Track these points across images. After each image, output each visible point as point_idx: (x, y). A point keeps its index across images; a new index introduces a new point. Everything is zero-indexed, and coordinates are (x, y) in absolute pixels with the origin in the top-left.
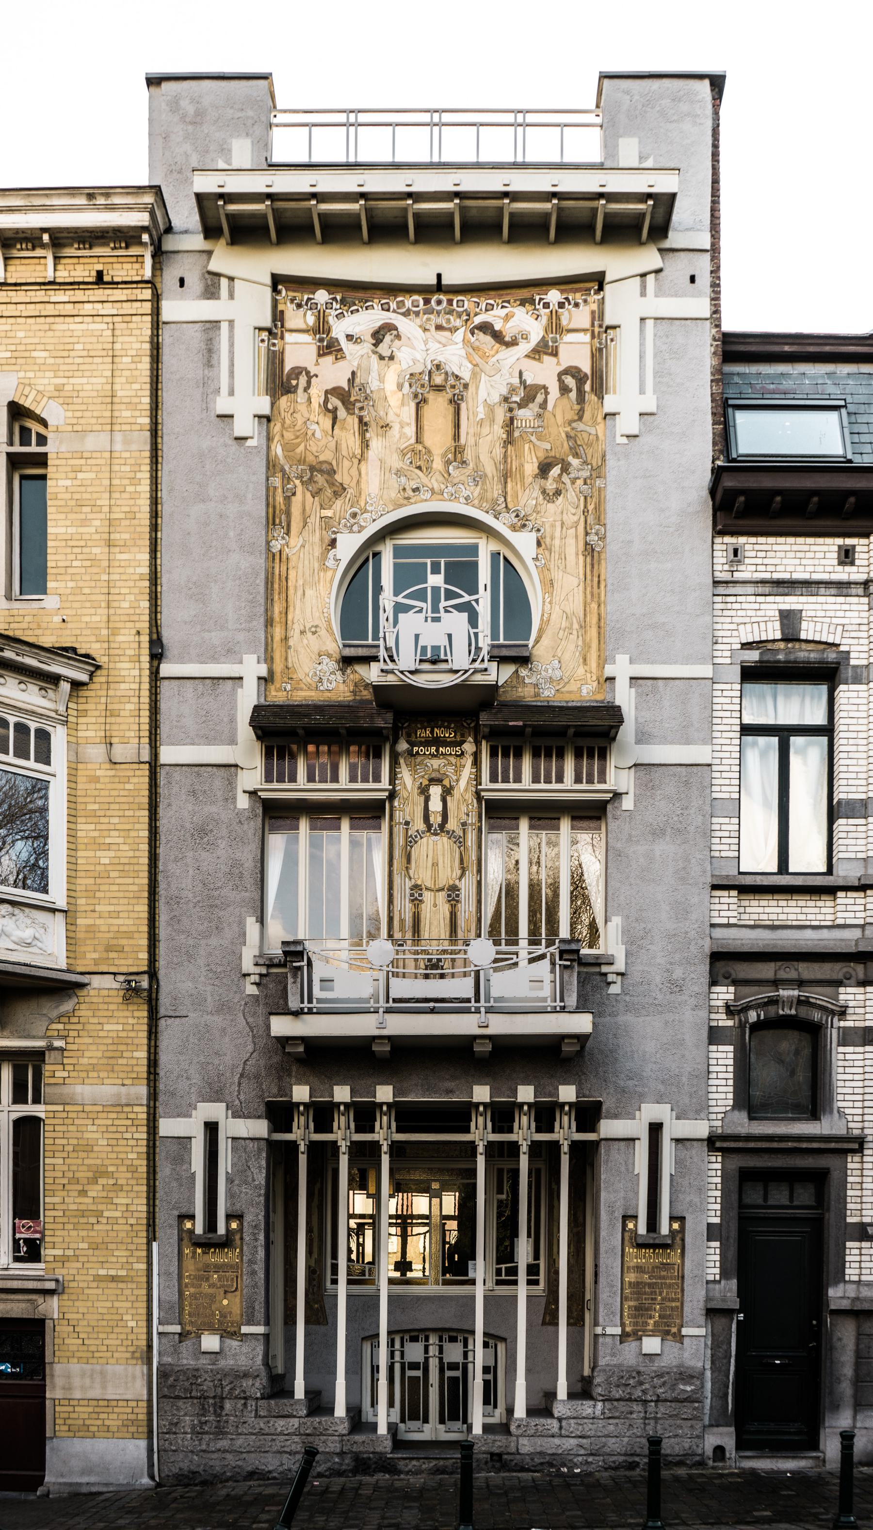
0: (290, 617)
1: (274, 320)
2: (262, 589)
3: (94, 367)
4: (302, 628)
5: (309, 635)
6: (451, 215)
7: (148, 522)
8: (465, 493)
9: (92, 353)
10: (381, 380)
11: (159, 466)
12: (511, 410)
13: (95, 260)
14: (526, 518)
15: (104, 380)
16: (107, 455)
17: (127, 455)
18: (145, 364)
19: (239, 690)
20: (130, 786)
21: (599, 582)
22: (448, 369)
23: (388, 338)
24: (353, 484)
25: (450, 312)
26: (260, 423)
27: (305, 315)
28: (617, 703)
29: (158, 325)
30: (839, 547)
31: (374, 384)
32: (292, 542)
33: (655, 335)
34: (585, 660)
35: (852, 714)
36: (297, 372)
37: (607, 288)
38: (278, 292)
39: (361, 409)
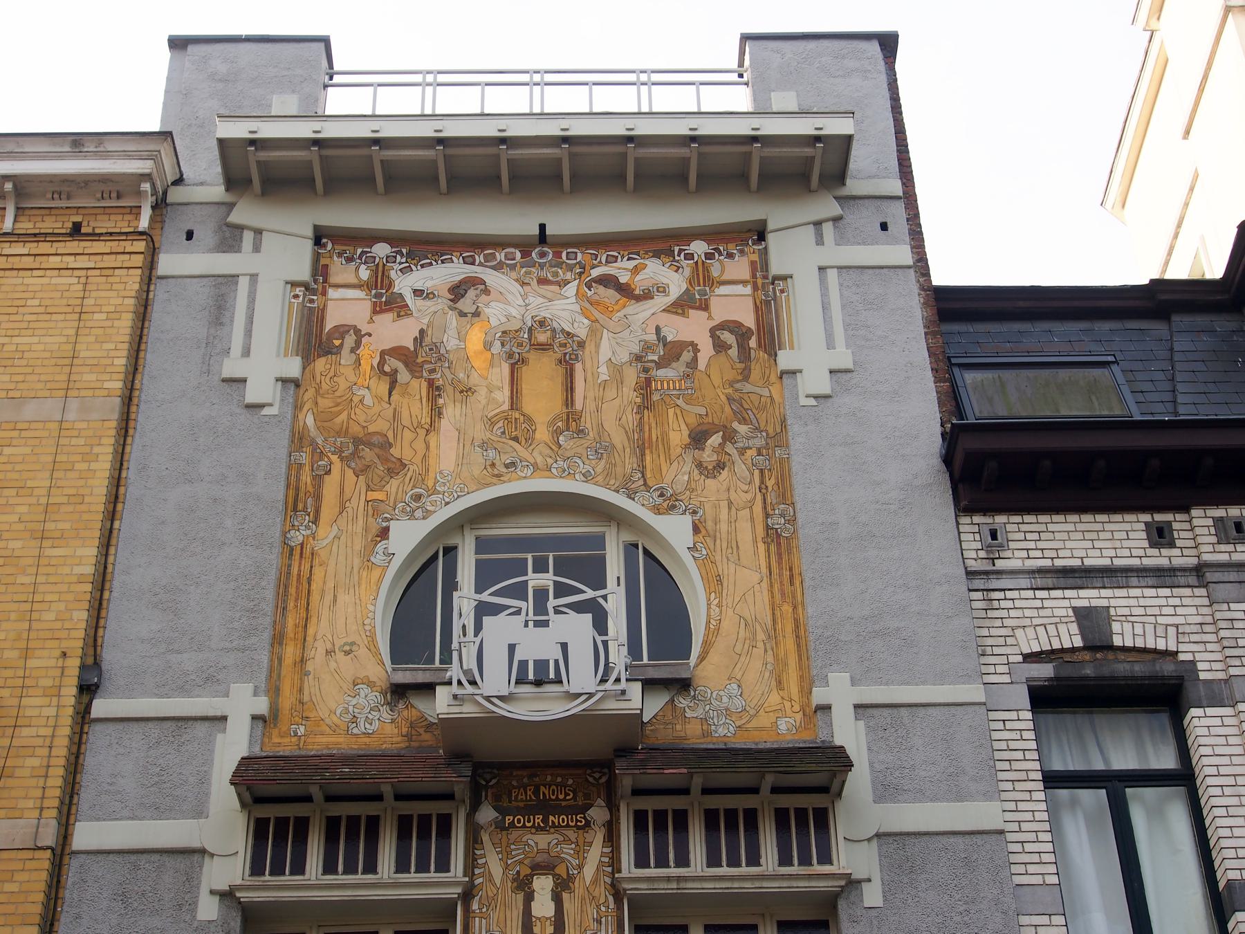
0: (311, 631)
1: (314, 274)
2: (270, 594)
3: (52, 325)
4: (329, 646)
5: (340, 656)
6: (559, 161)
7: (101, 507)
8: (583, 468)
9: (50, 310)
10: (462, 337)
11: (129, 440)
12: (646, 370)
13: (74, 211)
14: (675, 497)
15: (64, 339)
16: (55, 426)
17: (84, 425)
18: (125, 323)
19: (220, 737)
20: (13, 887)
21: (792, 577)
22: (555, 325)
23: (471, 293)
24: (418, 459)
25: (559, 265)
26: (284, 388)
27: (357, 269)
28: (838, 742)
29: (150, 279)
30: (1146, 523)
31: (451, 342)
32: (321, 532)
33: (841, 285)
34: (779, 683)
35: (1218, 750)
36: (342, 331)
37: (771, 238)
38: (325, 246)
39: (432, 371)
